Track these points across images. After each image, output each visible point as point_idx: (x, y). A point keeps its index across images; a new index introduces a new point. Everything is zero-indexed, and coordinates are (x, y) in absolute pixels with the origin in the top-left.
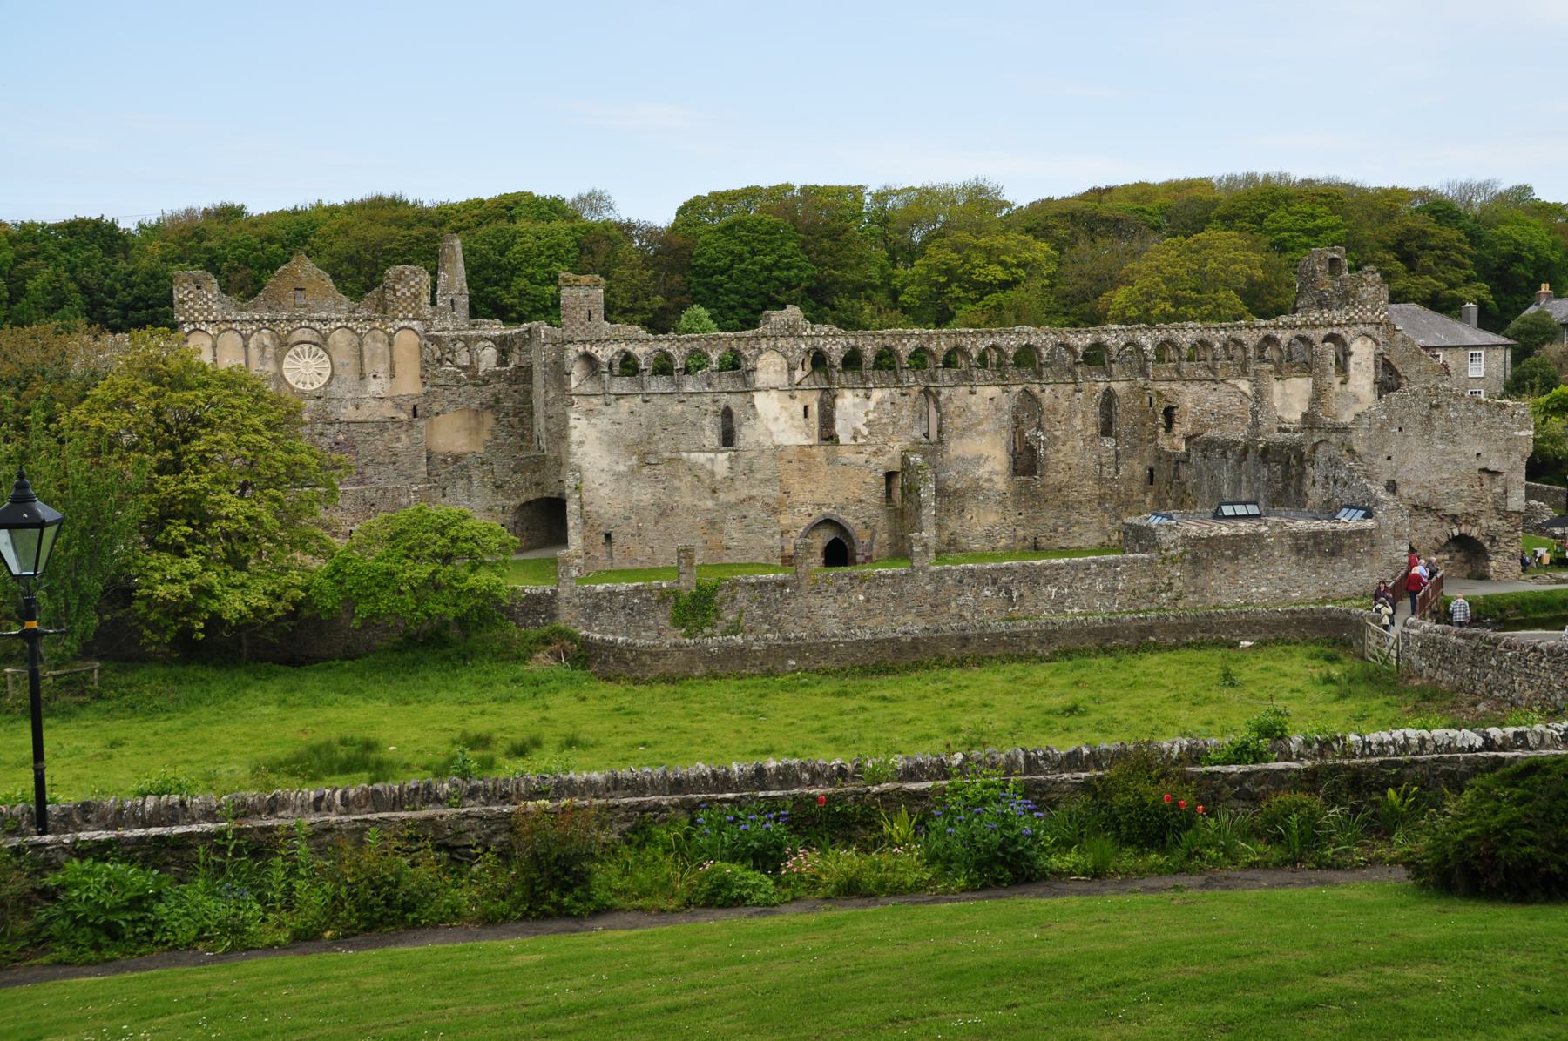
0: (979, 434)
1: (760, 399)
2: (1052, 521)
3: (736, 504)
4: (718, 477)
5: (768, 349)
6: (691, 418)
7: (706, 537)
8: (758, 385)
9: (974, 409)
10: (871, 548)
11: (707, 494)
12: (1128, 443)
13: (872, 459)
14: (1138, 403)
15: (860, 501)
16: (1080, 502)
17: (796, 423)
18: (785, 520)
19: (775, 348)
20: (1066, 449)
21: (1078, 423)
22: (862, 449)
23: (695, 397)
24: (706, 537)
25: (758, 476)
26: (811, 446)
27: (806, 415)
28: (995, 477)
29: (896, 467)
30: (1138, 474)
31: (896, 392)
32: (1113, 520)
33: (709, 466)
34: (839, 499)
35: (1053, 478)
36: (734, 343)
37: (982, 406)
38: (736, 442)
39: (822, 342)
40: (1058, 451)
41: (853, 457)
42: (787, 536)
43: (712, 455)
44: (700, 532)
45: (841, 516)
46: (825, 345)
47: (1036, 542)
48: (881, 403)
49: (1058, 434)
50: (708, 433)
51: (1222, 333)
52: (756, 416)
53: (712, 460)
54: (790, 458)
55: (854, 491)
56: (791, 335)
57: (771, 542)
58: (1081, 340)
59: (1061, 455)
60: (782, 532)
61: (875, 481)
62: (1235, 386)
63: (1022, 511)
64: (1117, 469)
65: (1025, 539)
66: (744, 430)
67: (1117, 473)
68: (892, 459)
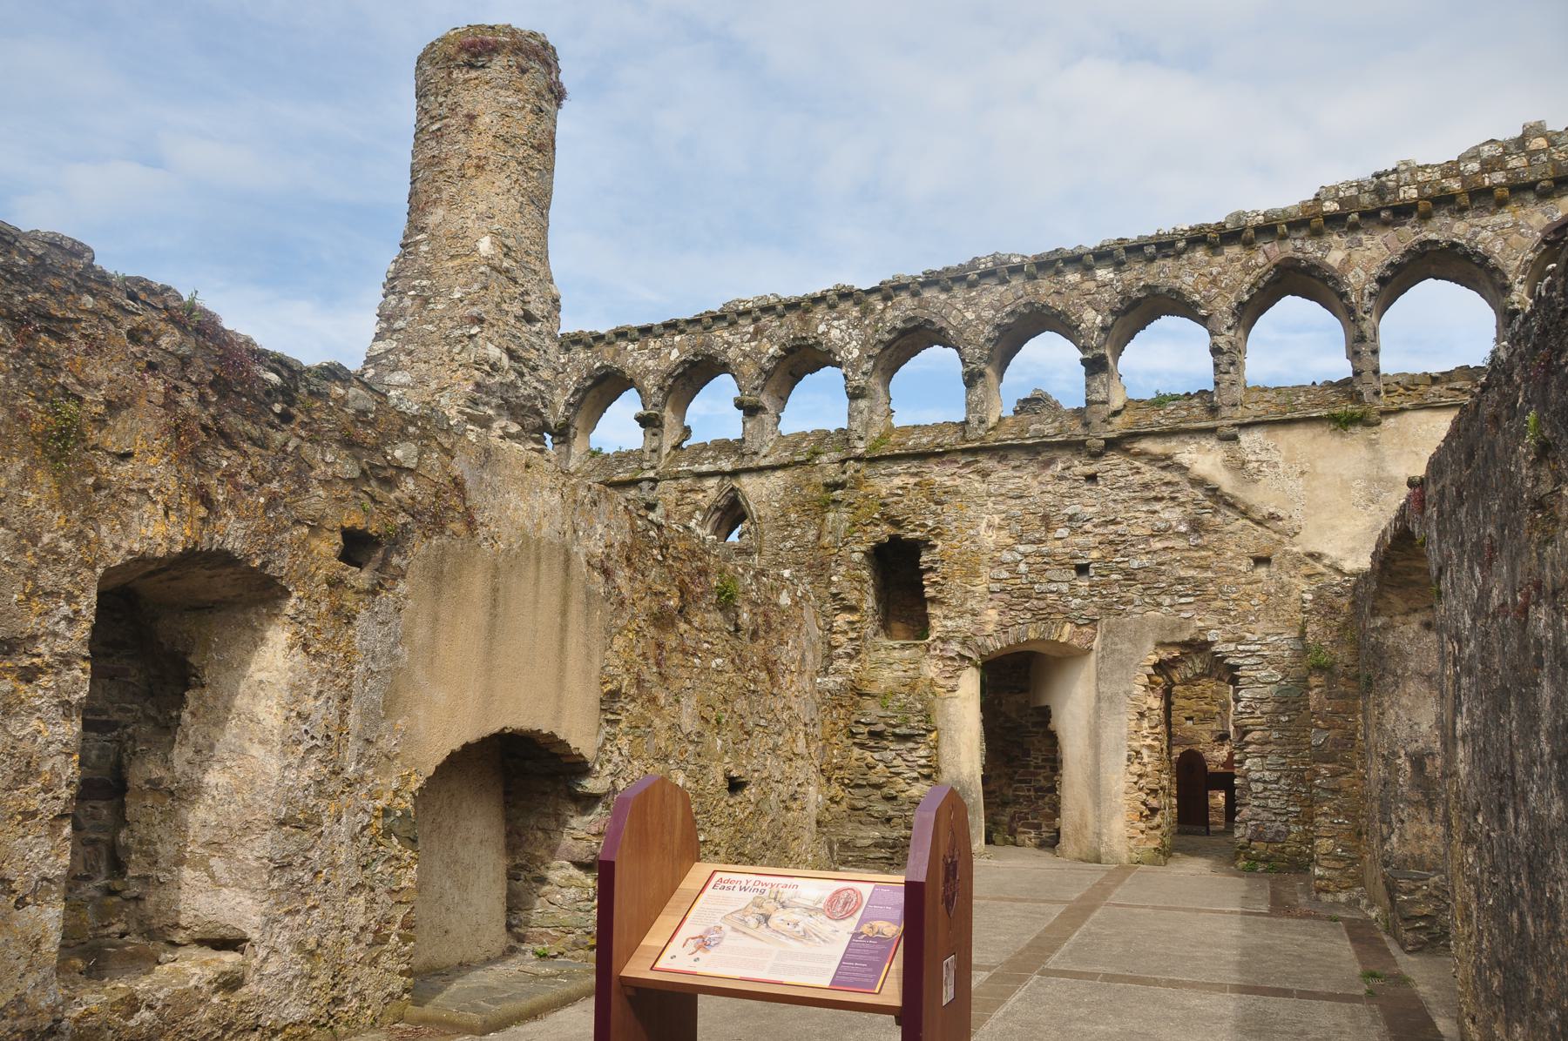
14: (811, 535)
51: (1104, 274)
58: (656, 353)
62: (1166, 462)
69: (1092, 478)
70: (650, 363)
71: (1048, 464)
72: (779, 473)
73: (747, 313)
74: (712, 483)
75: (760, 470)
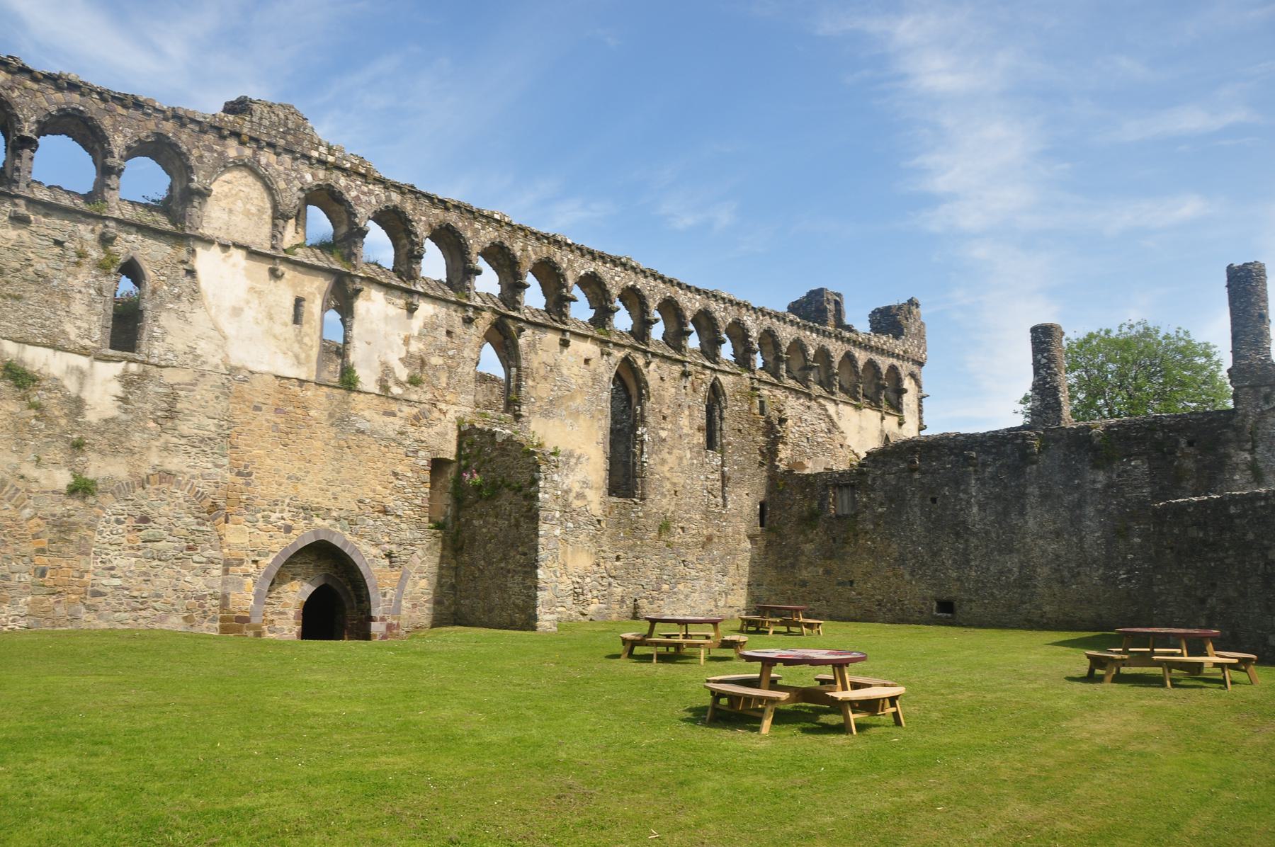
0: (571, 414)
1: (206, 261)
2: (657, 572)
3: (130, 487)
4: (92, 417)
5: (240, 165)
6: (40, 266)
7: (43, 560)
8: (206, 231)
9: (565, 371)
10: (397, 610)
11: (57, 453)
12: (735, 463)
13: (411, 429)
14: (746, 407)
15: (385, 511)
16: (687, 546)
17: (278, 329)
18: (237, 536)
19: (252, 168)
20: (671, 460)
21: (684, 421)
22: (394, 407)
23: (56, 222)
24: (43, 560)
25: (184, 428)
26: (302, 382)
27: (297, 319)
28: (588, 492)
29: (449, 450)
30: (747, 510)
31: (457, 317)
32: (720, 577)
33: (71, 386)
34: (347, 502)
35: (659, 502)
36: (168, 127)
37: (575, 370)
38: (144, 344)
39: (343, 181)
40: (663, 462)
41: (379, 421)
42: (237, 571)
43: (83, 362)
44: (28, 548)
45: (348, 537)
46: (348, 189)
47: (636, 607)
48: (430, 326)
49: (663, 434)
50: (78, 307)
51: (814, 335)
52: (195, 292)
53: (82, 375)
54: (259, 399)
55: (375, 488)
56: (288, 151)
57: (199, 584)
59: (666, 468)
60: (227, 564)
61: (415, 470)
63: (621, 553)
64: (724, 498)
65: (622, 601)
66: (164, 319)
67: (725, 506)
68: (442, 435)
69: (809, 407)
70: (688, 304)
71: (798, 398)
72: (731, 376)
73: (723, 299)
74: (708, 372)
75: (724, 372)
